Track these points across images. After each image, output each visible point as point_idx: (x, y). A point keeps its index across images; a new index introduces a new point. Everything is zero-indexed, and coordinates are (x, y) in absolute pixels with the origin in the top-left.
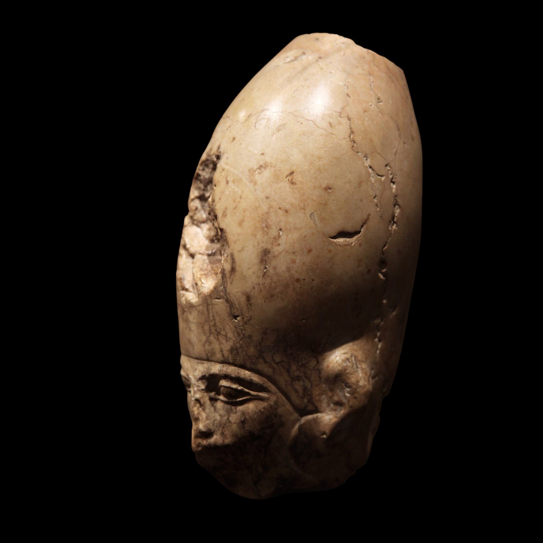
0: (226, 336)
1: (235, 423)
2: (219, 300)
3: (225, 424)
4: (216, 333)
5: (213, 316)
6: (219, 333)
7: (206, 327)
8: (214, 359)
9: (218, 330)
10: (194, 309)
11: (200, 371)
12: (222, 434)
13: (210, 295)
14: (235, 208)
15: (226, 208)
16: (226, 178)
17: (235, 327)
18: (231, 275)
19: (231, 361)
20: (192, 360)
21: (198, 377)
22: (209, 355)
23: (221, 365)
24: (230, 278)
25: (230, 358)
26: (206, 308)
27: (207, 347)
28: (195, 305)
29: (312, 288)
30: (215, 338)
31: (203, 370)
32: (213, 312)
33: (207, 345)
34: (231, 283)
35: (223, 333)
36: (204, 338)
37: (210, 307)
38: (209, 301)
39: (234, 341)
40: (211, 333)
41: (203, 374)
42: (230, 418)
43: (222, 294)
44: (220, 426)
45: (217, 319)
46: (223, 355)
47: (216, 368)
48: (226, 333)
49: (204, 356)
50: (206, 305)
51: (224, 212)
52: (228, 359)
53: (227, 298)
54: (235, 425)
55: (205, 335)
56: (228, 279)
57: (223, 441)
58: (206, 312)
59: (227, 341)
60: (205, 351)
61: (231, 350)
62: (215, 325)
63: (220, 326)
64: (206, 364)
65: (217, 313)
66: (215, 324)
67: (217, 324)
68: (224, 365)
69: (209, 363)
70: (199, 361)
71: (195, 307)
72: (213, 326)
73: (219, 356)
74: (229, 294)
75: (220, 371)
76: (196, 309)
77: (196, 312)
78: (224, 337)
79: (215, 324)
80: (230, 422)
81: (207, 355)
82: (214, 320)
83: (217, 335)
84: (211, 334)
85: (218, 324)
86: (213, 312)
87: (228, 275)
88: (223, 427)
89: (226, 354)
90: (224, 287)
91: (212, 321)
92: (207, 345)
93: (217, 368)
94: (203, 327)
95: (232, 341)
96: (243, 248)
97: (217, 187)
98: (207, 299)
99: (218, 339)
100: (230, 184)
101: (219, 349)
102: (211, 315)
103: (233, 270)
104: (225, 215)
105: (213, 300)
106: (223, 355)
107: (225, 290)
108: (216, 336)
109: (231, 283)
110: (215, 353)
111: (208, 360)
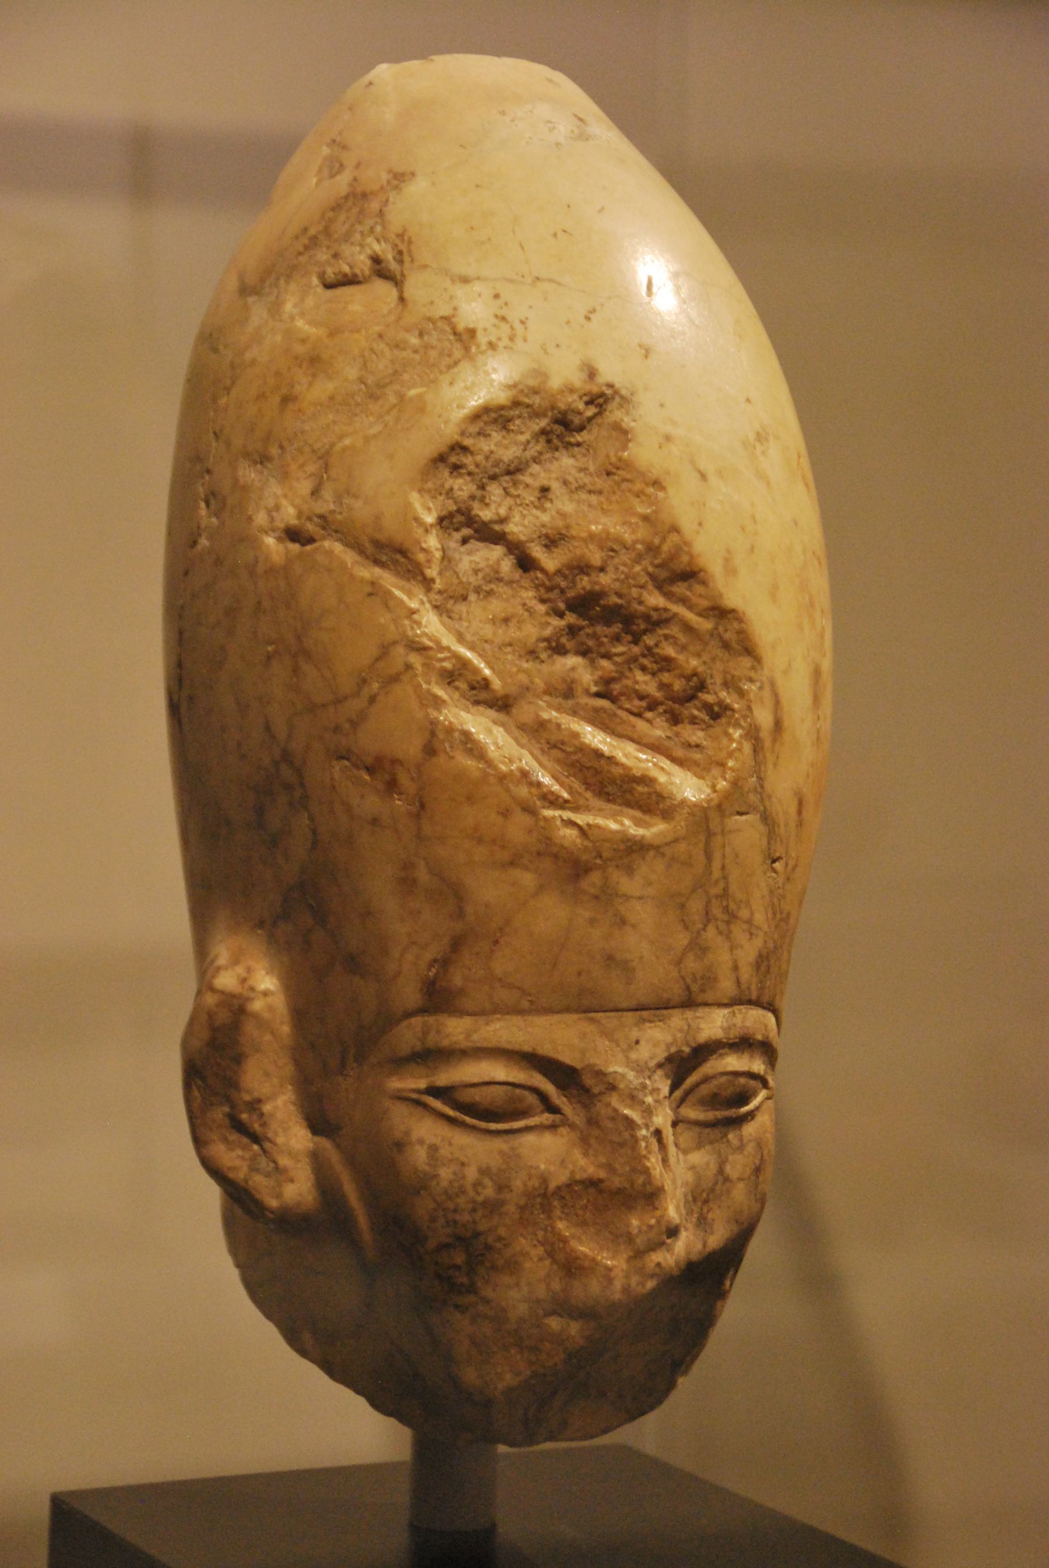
0: (749, 922)
1: (740, 1179)
2: (744, 818)
3: (713, 1190)
4: (726, 917)
5: (723, 867)
6: (732, 917)
7: (696, 906)
8: (709, 997)
9: (732, 906)
10: (652, 853)
11: (656, 1044)
12: (703, 1223)
13: (719, 806)
14: (752, 549)
15: (729, 551)
16: (692, 462)
17: (771, 892)
18: (774, 741)
19: (754, 996)
20: (609, 1020)
21: (652, 1064)
22: (695, 988)
23: (726, 1011)
24: (773, 750)
25: (753, 987)
26: (701, 845)
27: (691, 964)
28: (657, 842)
29: (808, 776)
30: (721, 933)
31: (669, 1039)
32: (724, 856)
33: (691, 957)
34: (775, 765)
35: (744, 913)
36: (682, 939)
37: (718, 840)
38: (715, 824)
39: (766, 933)
40: (708, 917)
41: (673, 1050)
42: (728, 1169)
43: (753, 798)
44: (695, 1200)
45: (734, 874)
46: (738, 982)
47: (713, 1024)
48: (752, 913)
49: (677, 992)
50: (702, 838)
51: (727, 560)
52: (749, 989)
53: (765, 809)
54: (741, 1186)
55: (686, 928)
56: (768, 754)
57: (705, 1245)
58: (702, 858)
59: (751, 934)
60: (683, 978)
61: (757, 962)
62: (725, 894)
63: (739, 896)
64: (677, 1019)
65: (737, 856)
66: (725, 889)
67: (730, 892)
68: (736, 1008)
69: (689, 1014)
70: (645, 1014)
71: (657, 848)
72: (717, 897)
73: (726, 986)
74: (769, 797)
75: (726, 1030)
76: (663, 855)
77: (660, 865)
78: (745, 926)
79: (725, 889)
80: (727, 1179)
81: (688, 988)
82: (725, 878)
83: (728, 923)
84: (709, 921)
85: (733, 888)
86: (724, 856)
87: (767, 743)
88: (706, 1201)
89: (746, 973)
90: (760, 778)
91: (717, 882)
92: (691, 957)
93: (719, 1024)
94: (683, 906)
95: (761, 934)
96: (790, 665)
97: (671, 491)
98: (707, 819)
99: (728, 936)
100: (713, 479)
101: (730, 964)
102: (716, 864)
103: (778, 726)
104: (731, 570)
105: (727, 821)
106: (738, 982)
107: (762, 787)
108: (722, 926)
109: (775, 765)
110: (715, 979)
111: (689, 1003)
